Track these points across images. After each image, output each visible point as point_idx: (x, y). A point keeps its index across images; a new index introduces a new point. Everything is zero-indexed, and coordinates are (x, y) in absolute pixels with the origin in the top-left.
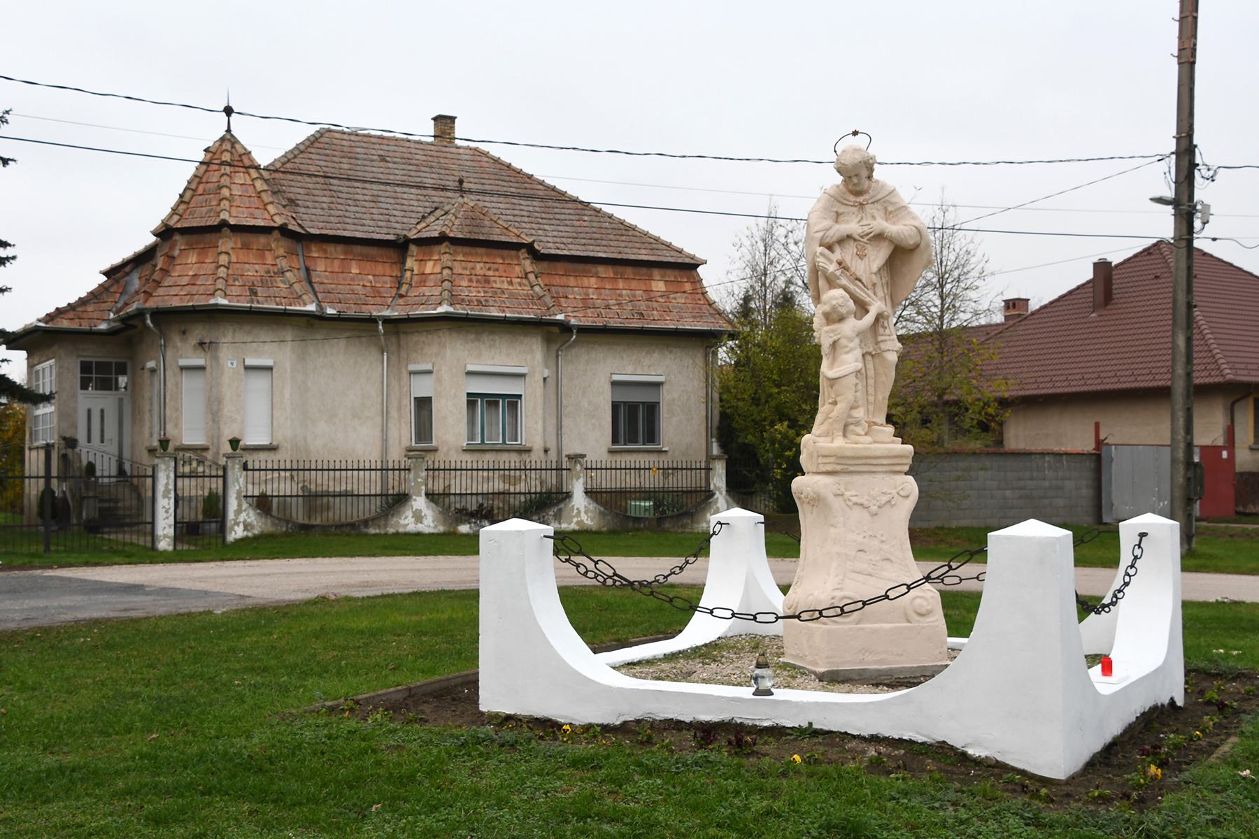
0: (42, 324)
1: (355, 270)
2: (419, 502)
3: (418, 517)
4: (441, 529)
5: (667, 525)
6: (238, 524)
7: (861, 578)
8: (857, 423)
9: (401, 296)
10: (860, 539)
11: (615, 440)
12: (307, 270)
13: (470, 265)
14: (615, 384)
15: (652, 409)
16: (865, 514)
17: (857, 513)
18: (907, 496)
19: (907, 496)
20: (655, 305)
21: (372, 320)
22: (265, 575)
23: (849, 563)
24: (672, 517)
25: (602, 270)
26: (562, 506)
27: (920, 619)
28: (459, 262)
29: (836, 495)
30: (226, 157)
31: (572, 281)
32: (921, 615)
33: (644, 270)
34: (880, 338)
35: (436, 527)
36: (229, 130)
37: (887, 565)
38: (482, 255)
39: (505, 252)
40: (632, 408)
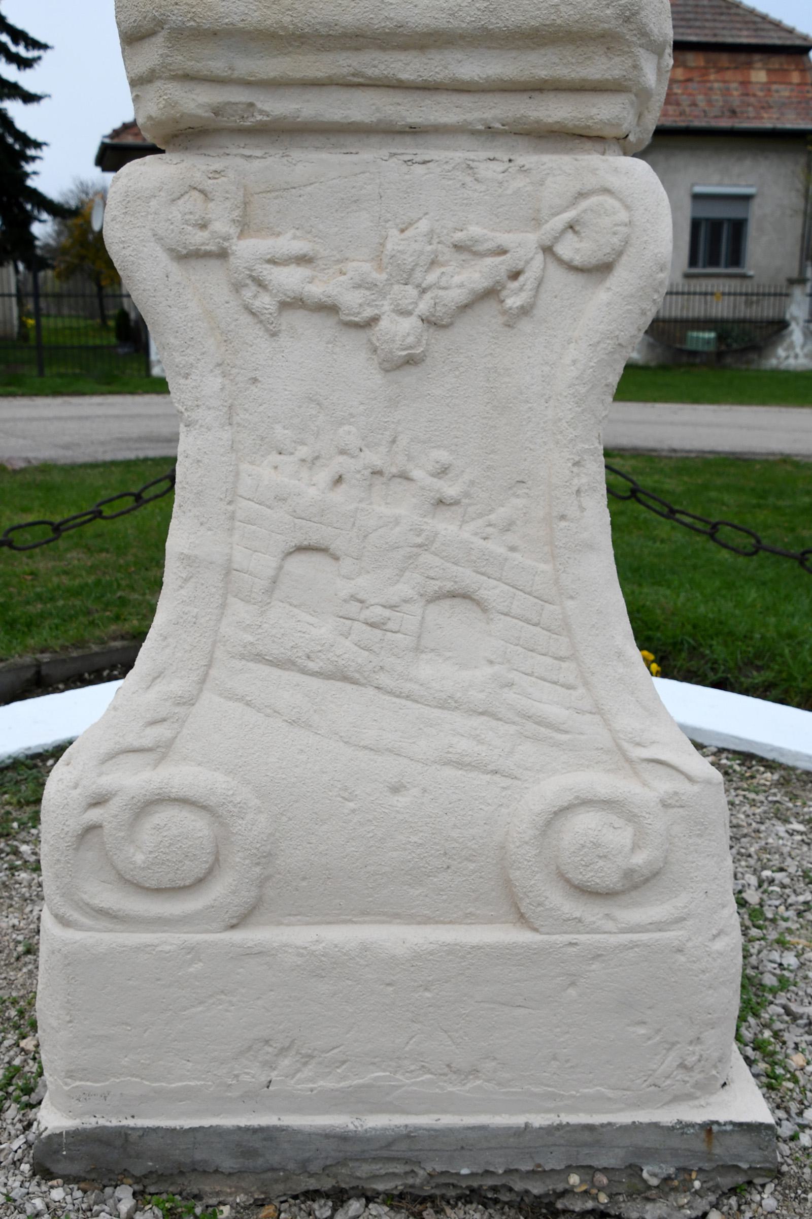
0: (107, 141)
7: (288, 691)
10: (312, 488)
11: (693, 262)
14: (697, 198)
15: (738, 227)
17: (308, 348)
18: (601, 269)
20: (752, 100)
22: (87, 418)
23: (240, 610)
24: (736, 351)
27: (592, 912)
29: (187, 256)
32: (586, 892)
33: (742, 58)
37: (448, 620)
40: (716, 225)
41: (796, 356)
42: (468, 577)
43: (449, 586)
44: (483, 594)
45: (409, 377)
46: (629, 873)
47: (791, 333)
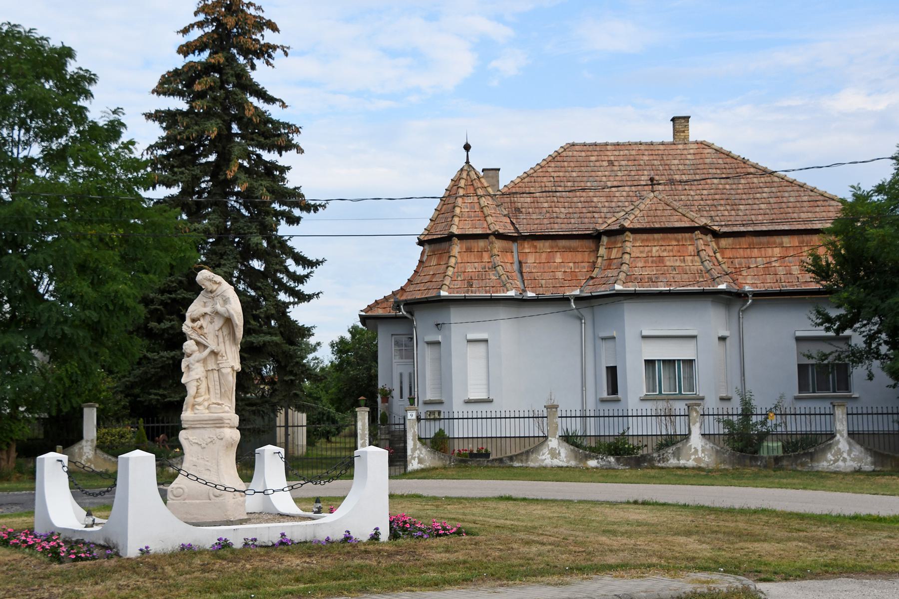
1: (558, 260)
2: (553, 443)
3: (554, 454)
4: (573, 463)
5: (785, 463)
6: (414, 458)
8: (199, 404)
9: (592, 278)
11: (802, 387)
12: (520, 263)
13: (647, 249)
14: (799, 339)
16: (199, 448)
21: (565, 300)
25: (786, 240)
26: (679, 445)
28: (656, 247)
30: (469, 183)
31: (755, 252)
35: (568, 461)
36: (468, 162)
38: (658, 240)
39: (679, 236)
41: (844, 460)
47: (838, 442)
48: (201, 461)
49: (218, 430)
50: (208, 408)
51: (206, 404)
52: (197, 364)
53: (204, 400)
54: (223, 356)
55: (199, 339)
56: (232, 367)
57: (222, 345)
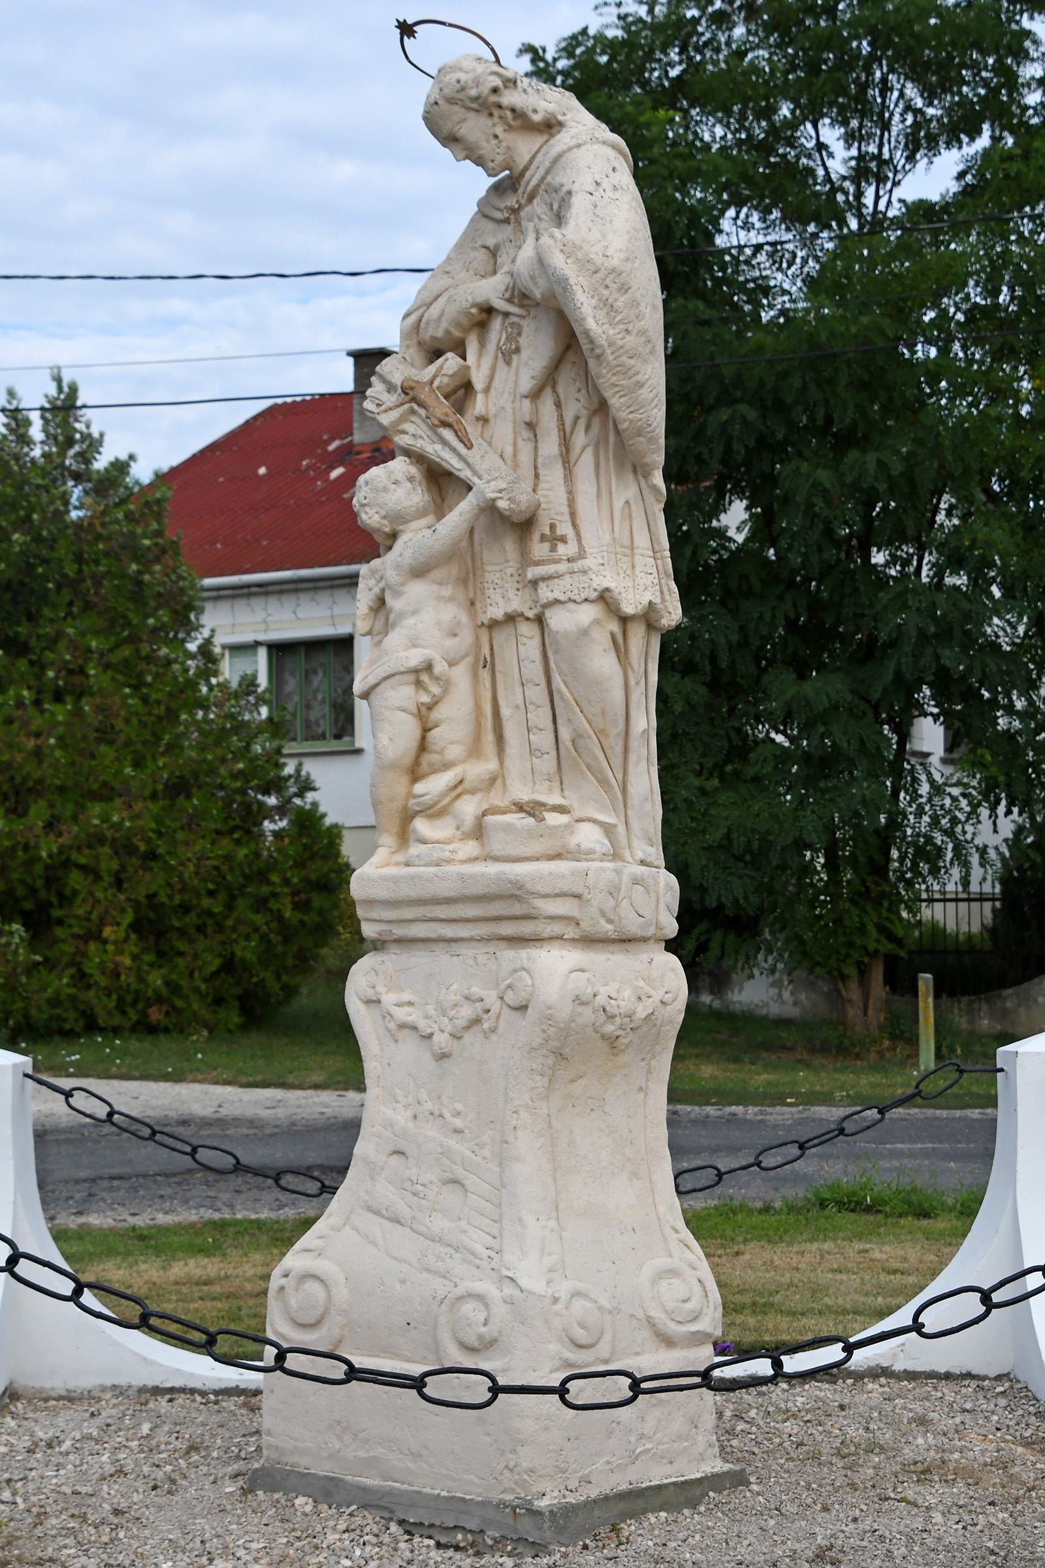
19: (522, 1008)
34: (532, 572)
42: (460, 1173)
43: (450, 1176)
44: (465, 1182)
45: (446, 1063)
46: (480, 1337)
48: (430, 1131)
49: (510, 956)
50: (478, 832)
51: (469, 808)
52: (417, 589)
53: (458, 788)
54: (555, 539)
55: (433, 450)
56: (605, 598)
57: (554, 476)
